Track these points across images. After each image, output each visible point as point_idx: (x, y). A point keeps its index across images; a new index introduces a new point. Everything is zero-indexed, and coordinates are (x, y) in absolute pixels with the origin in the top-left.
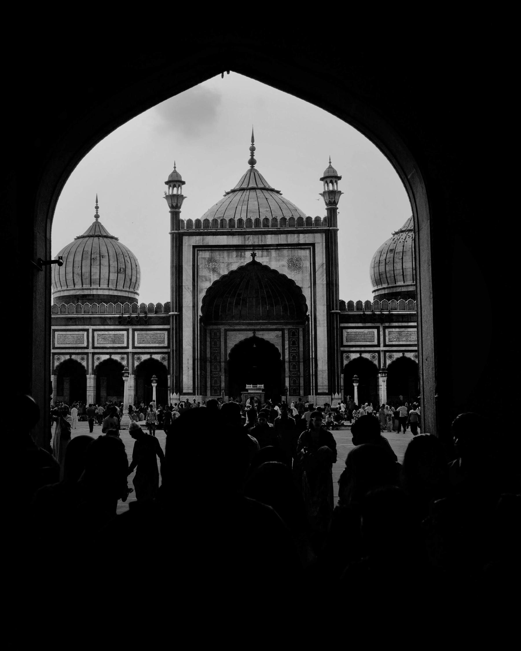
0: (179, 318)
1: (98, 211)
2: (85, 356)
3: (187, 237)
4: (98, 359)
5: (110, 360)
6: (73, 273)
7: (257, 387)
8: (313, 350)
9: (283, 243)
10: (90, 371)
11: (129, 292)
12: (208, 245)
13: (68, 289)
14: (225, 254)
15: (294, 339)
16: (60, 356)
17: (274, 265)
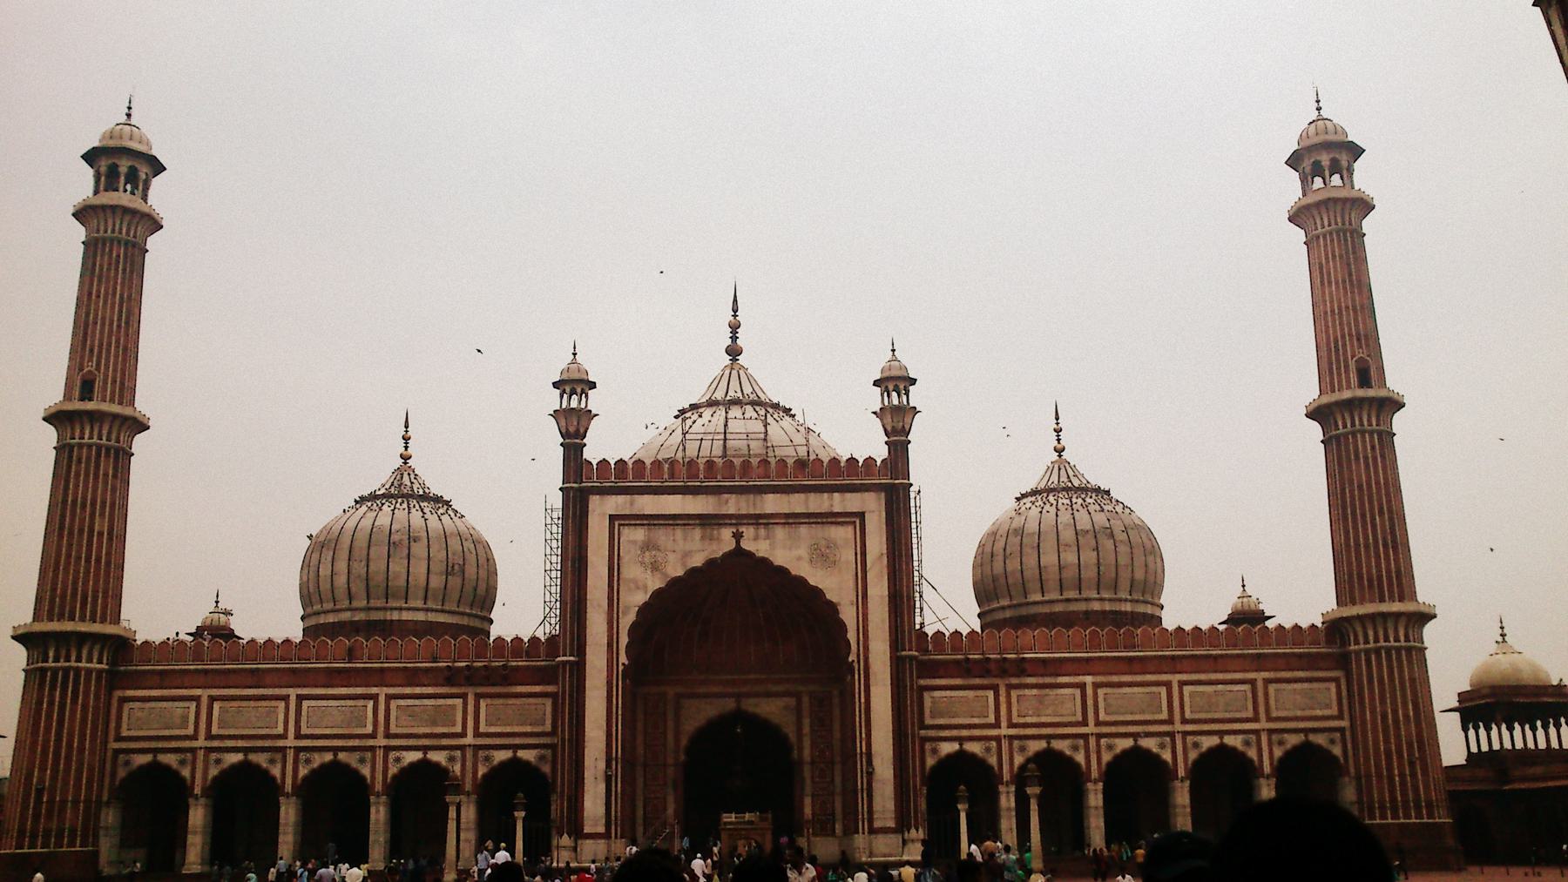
0: (578, 670)
3: (598, 496)
4: (398, 760)
5: (424, 763)
6: (349, 573)
8: (864, 736)
9: (798, 510)
10: (379, 787)
11: (469, 615)
13: (337, 607)
14: (679, 532)
17: (780, 558)
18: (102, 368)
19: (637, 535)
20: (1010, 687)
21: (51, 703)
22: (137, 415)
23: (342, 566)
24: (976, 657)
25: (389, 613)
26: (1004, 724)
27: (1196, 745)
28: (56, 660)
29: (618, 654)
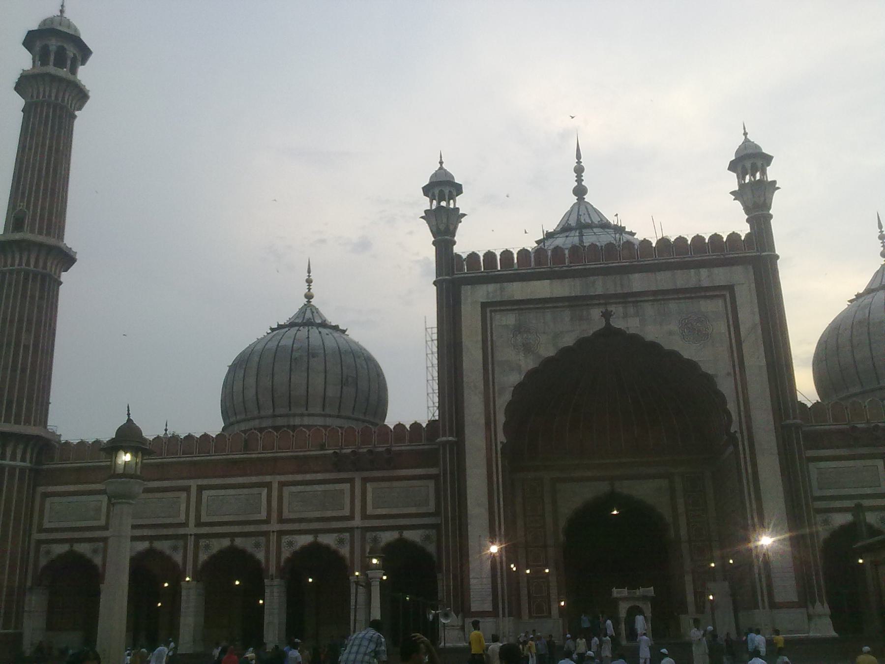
1: (311, 287)
2: (262, 540)
4: (290, 544)
7: (635, 593)
10: (273, 570)
12: (513, 299)
14: (548, 316)
16: (210, 540)
17: (652, 333)
18: (32, 208)
19: (510, 319)
22: (61, 245)
29: (496, 435)
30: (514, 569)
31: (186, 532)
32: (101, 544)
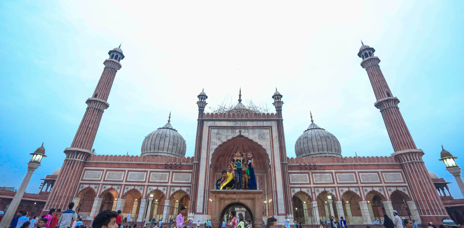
2: (143, 187)
14: (225, 131)
15: (262, 181)
16: (129, 186)
17: (251, 137)
19: (216, 131)
20: (312, 173)
21: (66, 169)
23: (149, 142)
24: (303, 164)
25: (158, 153)
26: (312, 183)
27: (366, 190)
28: (71, 158)
30: (210, 199)
31: (122, 184)
32: (98, 186)
